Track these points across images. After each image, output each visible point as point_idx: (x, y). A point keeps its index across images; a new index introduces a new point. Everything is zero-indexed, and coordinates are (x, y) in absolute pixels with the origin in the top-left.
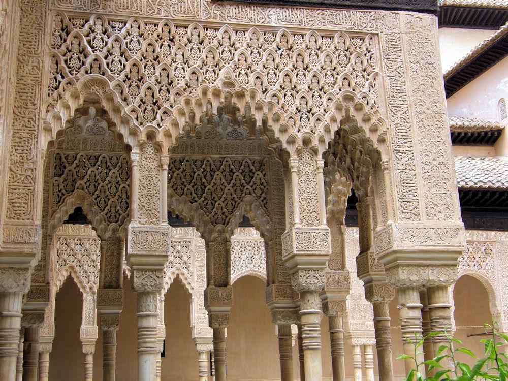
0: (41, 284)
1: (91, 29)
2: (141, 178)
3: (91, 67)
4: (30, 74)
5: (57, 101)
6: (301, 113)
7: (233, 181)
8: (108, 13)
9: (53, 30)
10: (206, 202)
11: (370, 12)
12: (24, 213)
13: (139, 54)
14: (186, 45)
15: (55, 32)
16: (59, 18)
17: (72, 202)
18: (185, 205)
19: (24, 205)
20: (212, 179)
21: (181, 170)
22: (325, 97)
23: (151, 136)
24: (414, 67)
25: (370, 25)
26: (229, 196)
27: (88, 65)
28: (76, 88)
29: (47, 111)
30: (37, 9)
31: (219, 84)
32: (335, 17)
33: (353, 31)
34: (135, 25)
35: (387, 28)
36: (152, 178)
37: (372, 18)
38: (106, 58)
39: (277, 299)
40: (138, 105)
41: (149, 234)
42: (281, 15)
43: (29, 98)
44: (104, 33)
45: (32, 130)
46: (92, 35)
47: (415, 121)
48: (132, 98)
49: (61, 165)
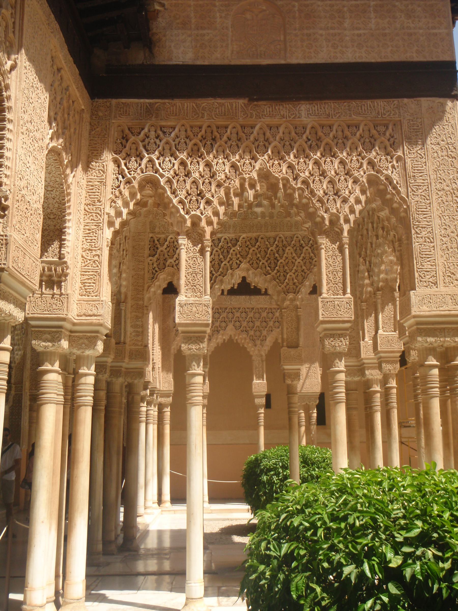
0: (140, 347)
1: (146, 135)
2: (187, 259)
7: (302, 255)
9: (115, 139)
10: (278, 274)
11: (393, 101)
12: (93, 291)
15: (117, 140)
17: (164, 278)
18: (260, 277)
19: (93, 284)
20: (284, 253)
24: (435, 148)
25: (393, 112)
26: (299, 268)
32: (360, 108)
33: (377, 119)
34: (183, 129)
35: (409, 114)
36: (197, 258)
40: (184, 197)
42: (311, 110)
44: (157, 138)
46: (147, 141)
47: (435, 197)
49: (155, 246)
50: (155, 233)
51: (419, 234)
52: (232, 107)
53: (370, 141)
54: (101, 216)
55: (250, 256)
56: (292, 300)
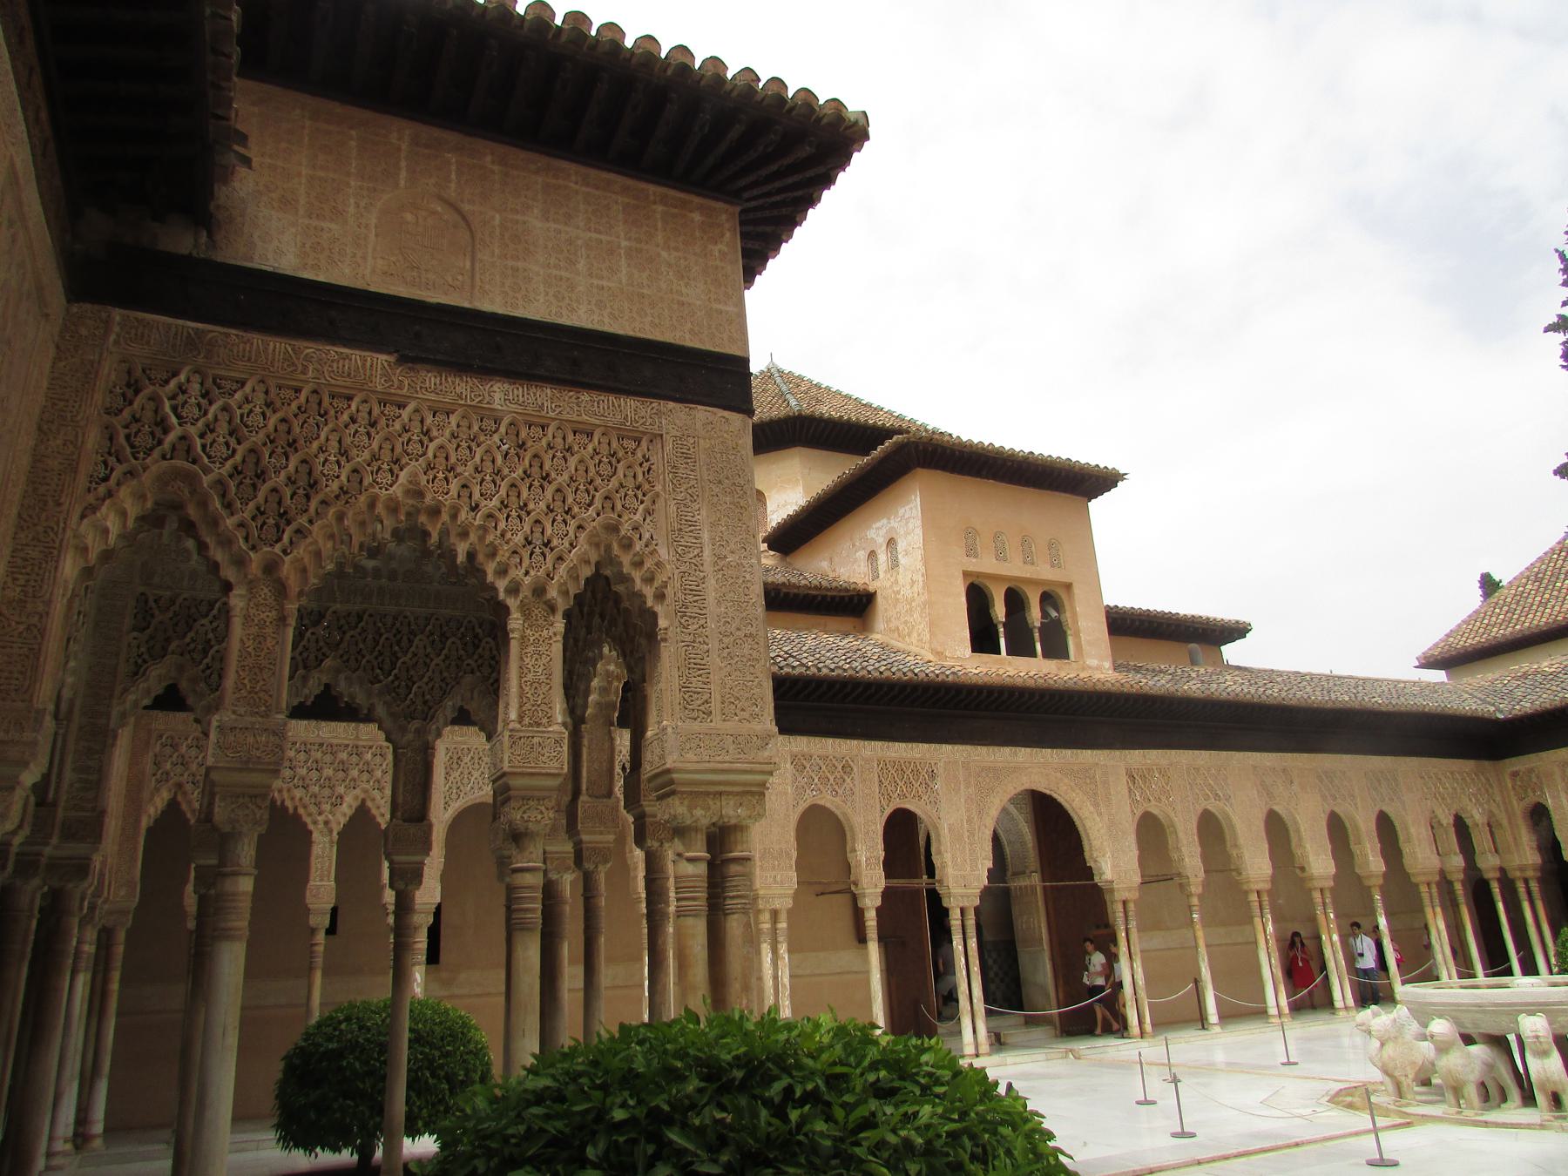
1: (180, 388)
3: (174, 448)
4: (59, 453)
5: (104, 500)
6: (532, 546)
7: (444, 652)
10: (396, 683)
11: (651, 403)
12: (16, 690)
13: (262, 435)
14: (346, 427)
15: (114, 387)
20: (411, 646)
21: (358, 630)
22: (573, 524)
23: (271, 567)
25: (650, 421)
29: (83, 516)
31: (397, 491)
34: (262, 388)
37: (654, 411)
44: (203, 396)
46: (181, 398)
51: (684, 627)
52: (364, 365)
53: (610, 462)
54: (56, 534)
55: (343, 646)
56: (417, 731)
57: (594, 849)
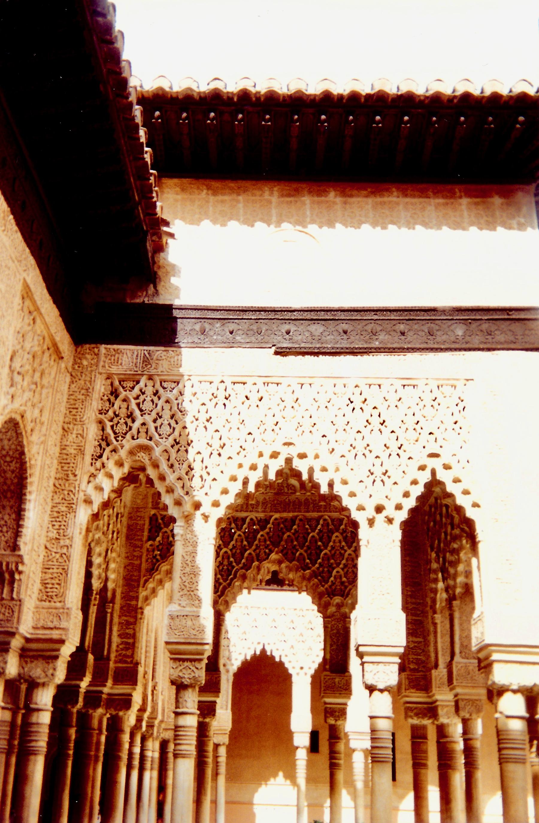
0: (129, 665)
2: (184, 554)
3: (139, 432)
5: (100, 470)
8: (160, 373)
9: (102, 394)
12: (56, 595)
15: (104, 396)
16: (109, 381)
17: (167, 571)
18: (296, 573)
27: (134, 431)
28: (119, 456)
29: (89, 482)
30: (87, 373)
38: (155, 421)
39: (408, 691)
41: (188, 619)
43: (71, 468)
44: (155, 394)
45: (71, 504)
46: (142, 398)
48: (179, 464)
50: (158, 508)
56: (339, 606)
57: (468, 700)
